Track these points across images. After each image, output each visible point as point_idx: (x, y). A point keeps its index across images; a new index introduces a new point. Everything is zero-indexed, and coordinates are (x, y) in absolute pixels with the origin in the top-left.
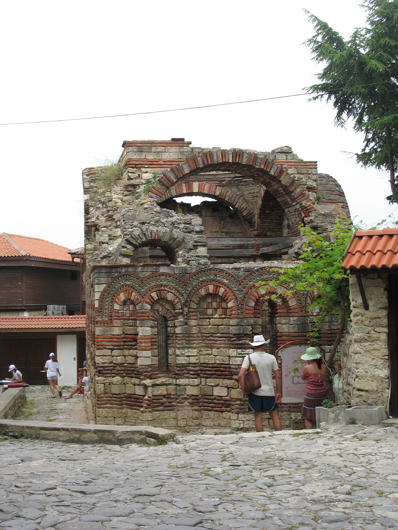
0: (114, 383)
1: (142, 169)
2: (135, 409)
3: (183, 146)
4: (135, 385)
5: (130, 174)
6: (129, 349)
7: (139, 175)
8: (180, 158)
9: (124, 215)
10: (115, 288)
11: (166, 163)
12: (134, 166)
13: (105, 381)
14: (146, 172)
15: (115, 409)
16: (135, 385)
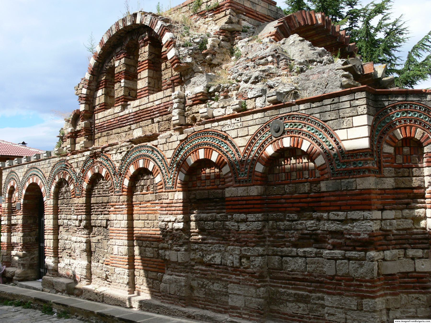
0: (388, 259)
1: (241, 15)
2: (415, 293)
3: (271, 4)
4: (413, 259)
5: (232, 17)
6: (402, 210)
7: (239, 21)
8: (269, 16)
9: (276, 50)
10: (384, 123)
11: (260, 16)
12: (235, 9)
13: (379, 258)
14: (244, 20)
15: (388, 297)
16: (413, 259)
